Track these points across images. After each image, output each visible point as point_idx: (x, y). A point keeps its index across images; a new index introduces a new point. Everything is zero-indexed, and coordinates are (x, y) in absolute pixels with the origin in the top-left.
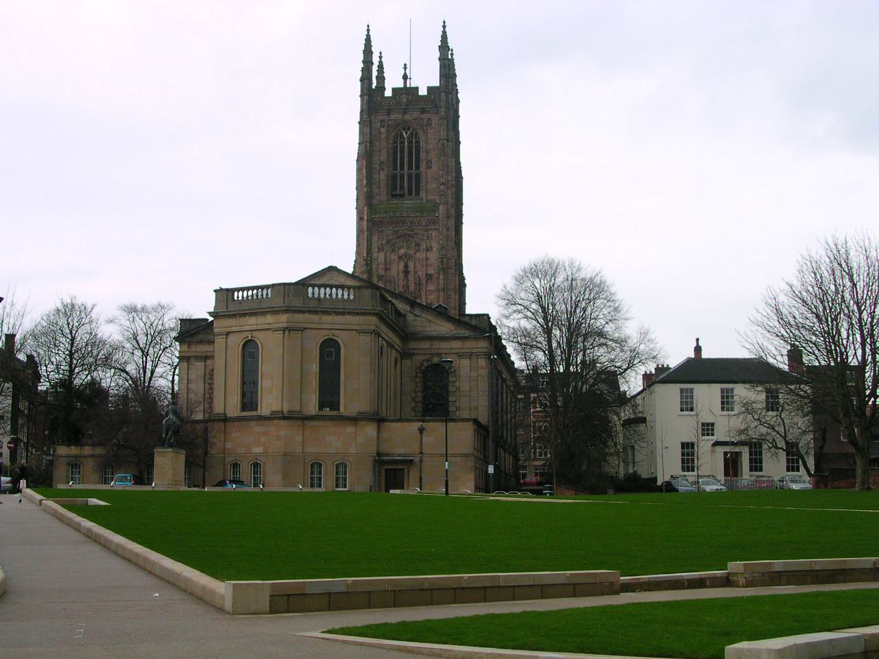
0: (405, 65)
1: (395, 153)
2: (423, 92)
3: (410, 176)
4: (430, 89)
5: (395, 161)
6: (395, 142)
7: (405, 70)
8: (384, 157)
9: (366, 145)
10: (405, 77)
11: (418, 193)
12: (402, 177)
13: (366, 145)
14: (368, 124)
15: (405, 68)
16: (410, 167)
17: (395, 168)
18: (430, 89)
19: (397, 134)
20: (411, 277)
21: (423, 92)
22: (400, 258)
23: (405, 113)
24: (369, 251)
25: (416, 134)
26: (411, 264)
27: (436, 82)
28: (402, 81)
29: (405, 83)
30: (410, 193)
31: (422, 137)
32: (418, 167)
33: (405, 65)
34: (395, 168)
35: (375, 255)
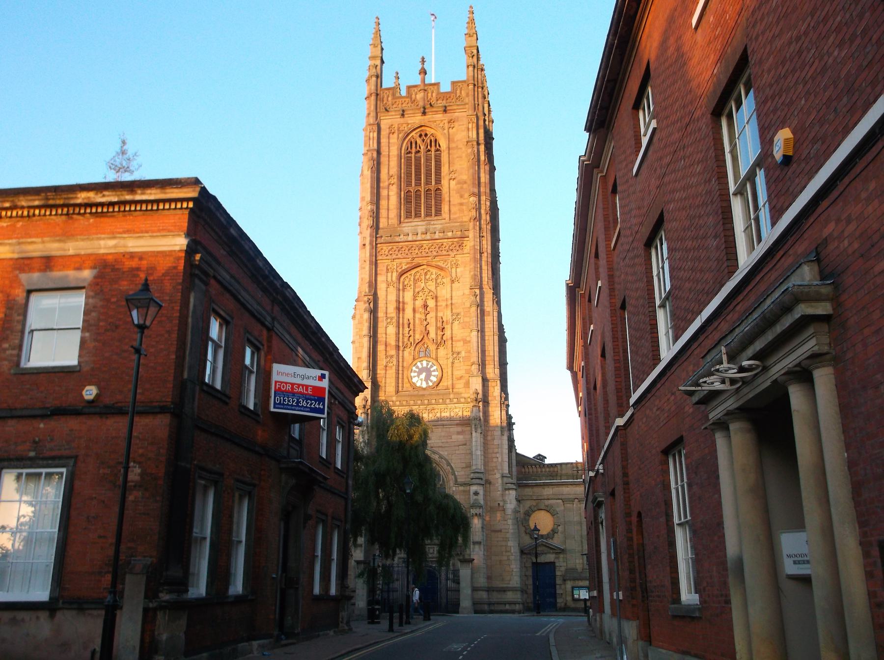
0: (423, 58)
1: (408, 165)
4: (454, 83)
5: (409, 174)
6: (410, 153)
8: (394, 171)
11: (438, 212)
14: (375, 128)
15: (423, 61)
16: (428, 182)
17: (409, 184)
18: (454, 83)
20: (431, 318)
23: (424, 113)
24: (373, 286)
25: (436, 141)
26: (431, 303)
27: (462, 73)
29: (423, 80)
31: (443, 144)
32: (438, 181)
33: (423, 58)
34: (409, 184)
35: (381, 294)
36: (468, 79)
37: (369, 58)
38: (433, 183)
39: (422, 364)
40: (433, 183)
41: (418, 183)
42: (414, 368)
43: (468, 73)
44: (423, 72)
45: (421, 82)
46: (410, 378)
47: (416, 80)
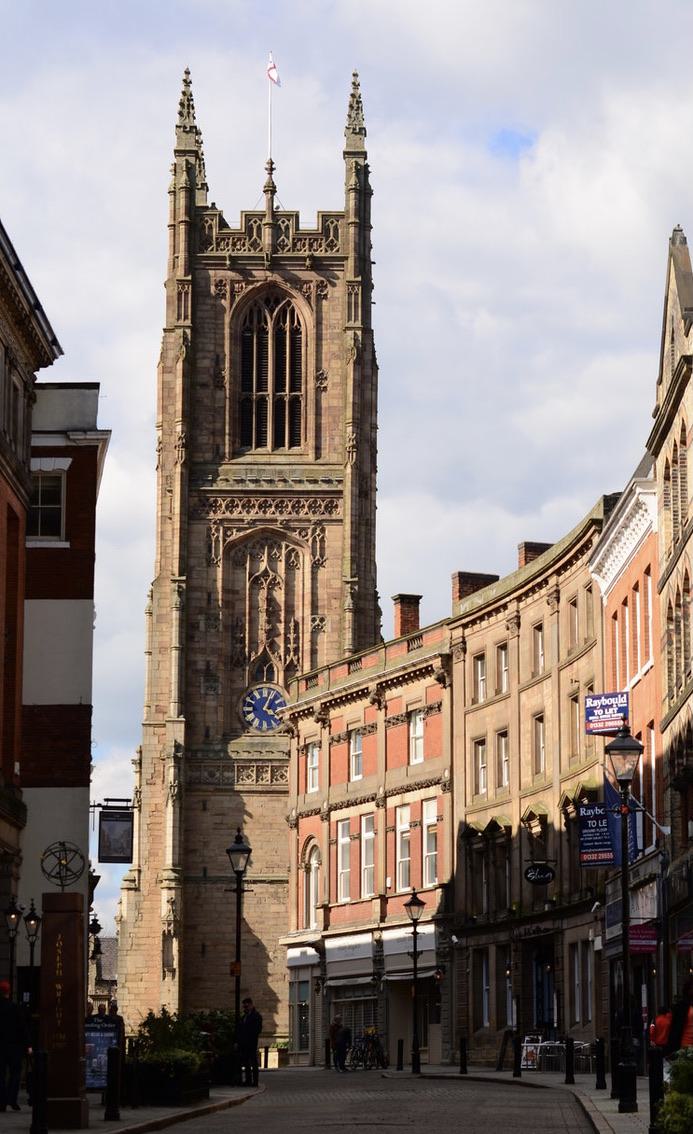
2: (309, 222)
3: (279, 404)
4: (325, 217)
7: (271, 174)
9: (184, 333)
10: (271, 190)
12: (262, 401)
13: (184, 333)
16: (279, 385)
18: (325, 217)
19: (251, 311)
21: (309, 222)
22: (256, 582)
27: (339, 200)
28: (265, 198)
30: (278, 443)
32: (295, 386)
36: (348, 211)
37: (176, 151)
38: (287, 391)
39: (261, 694)
40: (287, 391)
41: (262, 386)
42: (248, 700)
43: (347, 201)
44: (271, 190)
45: (268, 208)
46: (242, 716)
47: (260, 204)
